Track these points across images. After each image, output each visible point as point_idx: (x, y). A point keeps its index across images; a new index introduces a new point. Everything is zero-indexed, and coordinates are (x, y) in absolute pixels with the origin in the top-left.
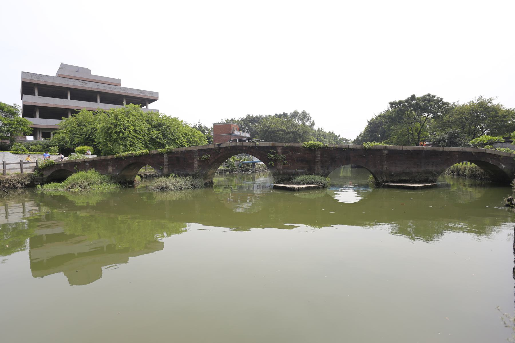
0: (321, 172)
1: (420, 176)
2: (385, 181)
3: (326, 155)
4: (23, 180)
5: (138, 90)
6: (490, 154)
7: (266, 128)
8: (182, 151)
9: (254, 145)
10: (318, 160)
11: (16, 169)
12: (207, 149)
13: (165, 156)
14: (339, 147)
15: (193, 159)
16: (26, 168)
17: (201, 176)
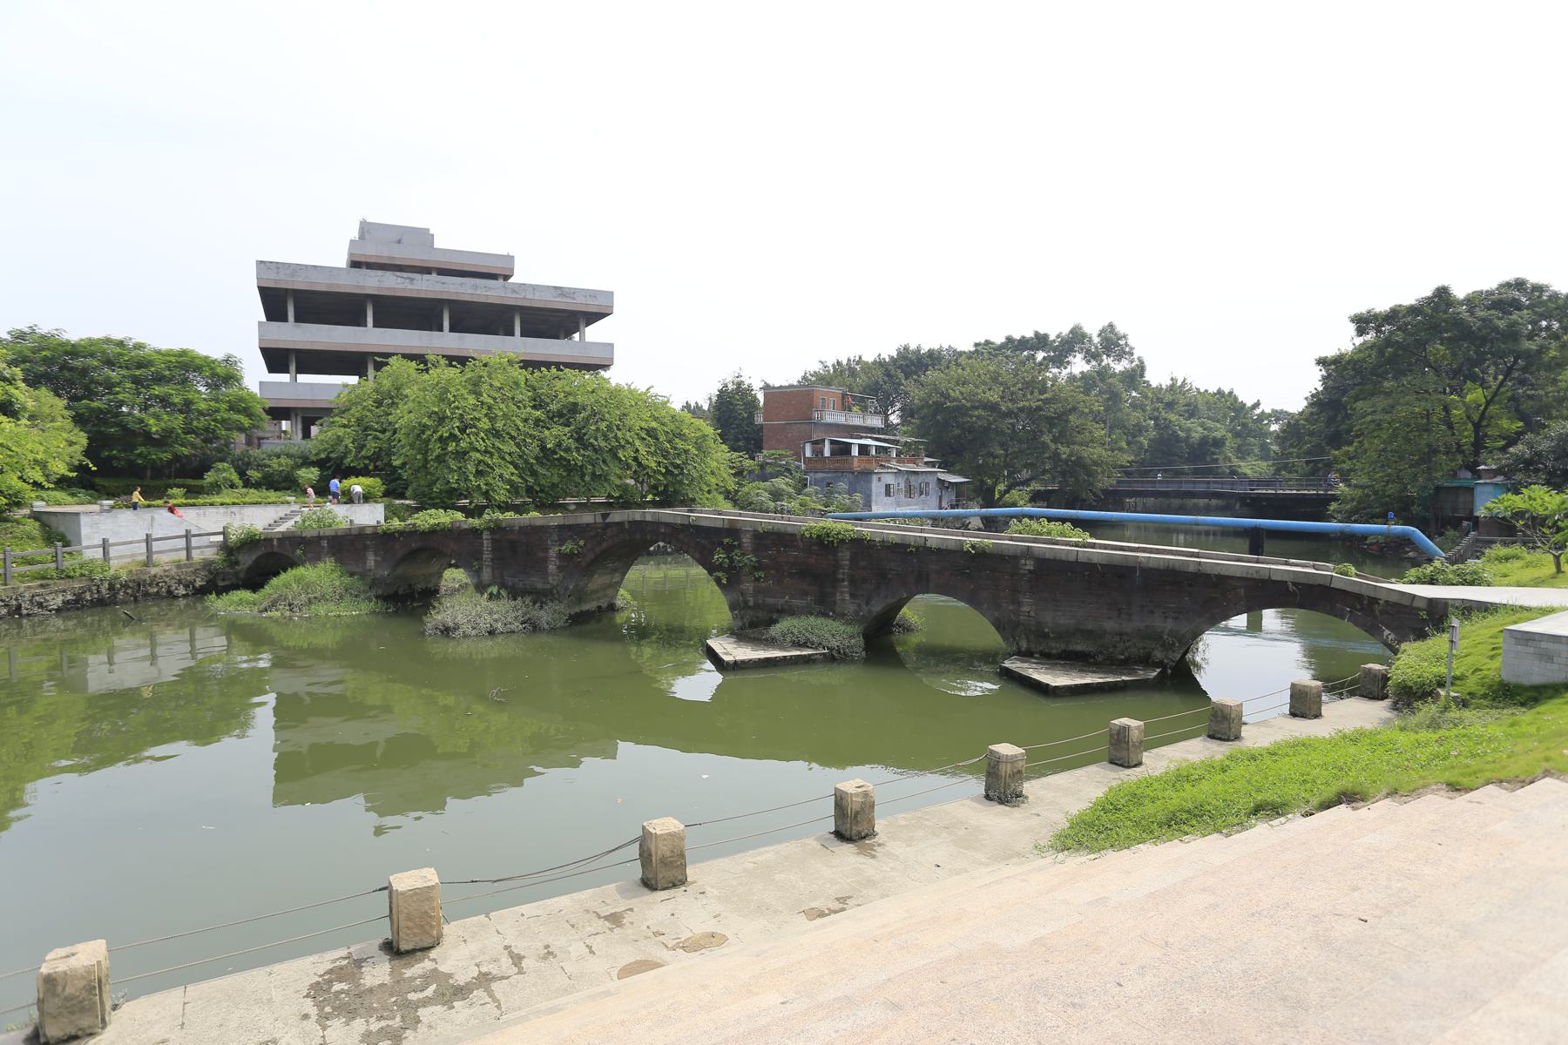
0: (851, 611)
1: (1128, 644)
2: (1023, 649)
3: (864, 563)
5: (555, 287)
6: (1345, 592)
7: (936, 398)
9: (686, 523)
10: (843, 573)
11: (177, 550)
12: (578, 526)
13: (486, 535)
15: (546, 550)
16: (199, 548)
17: (564, 595)
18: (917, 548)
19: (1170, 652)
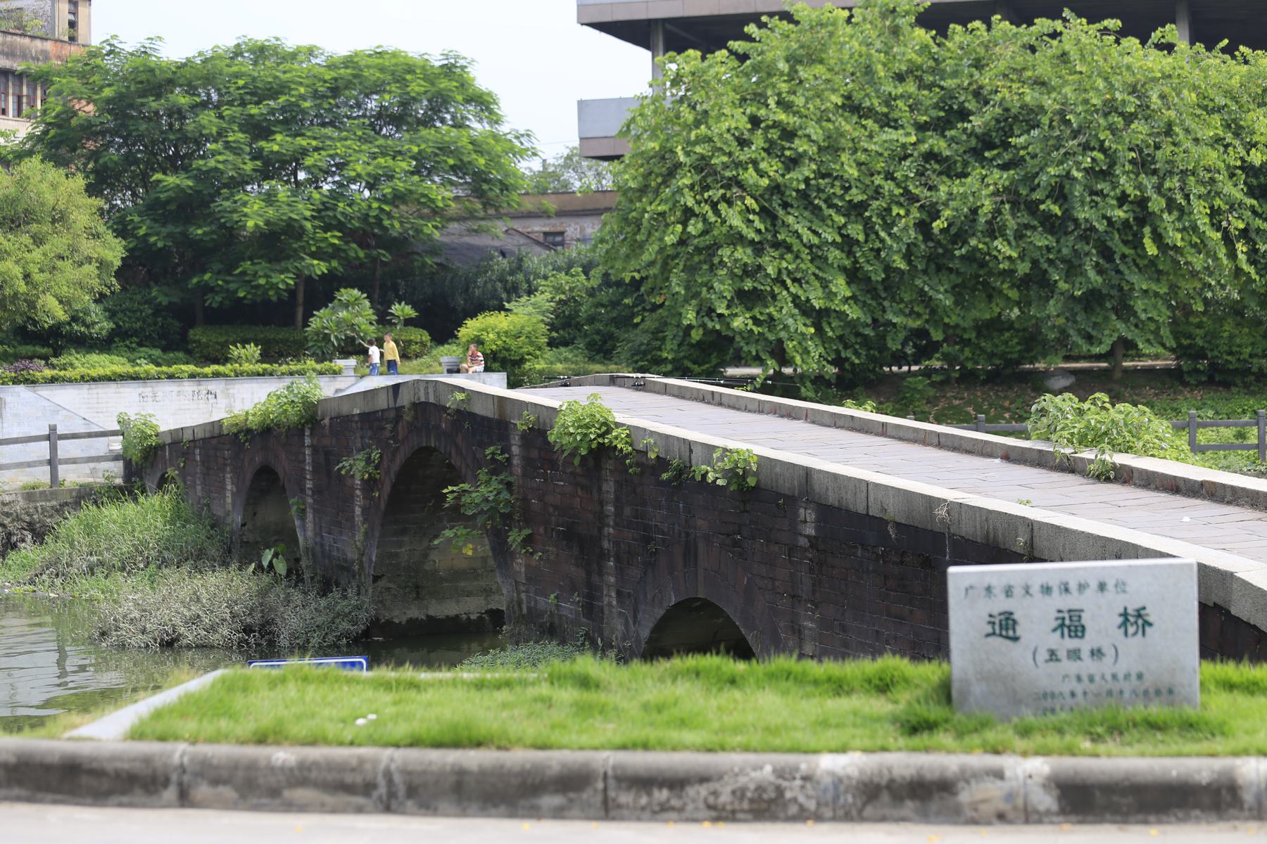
4: (51, 516)
8: (333, 416)
11: (29, 465)
16: (74, 461)
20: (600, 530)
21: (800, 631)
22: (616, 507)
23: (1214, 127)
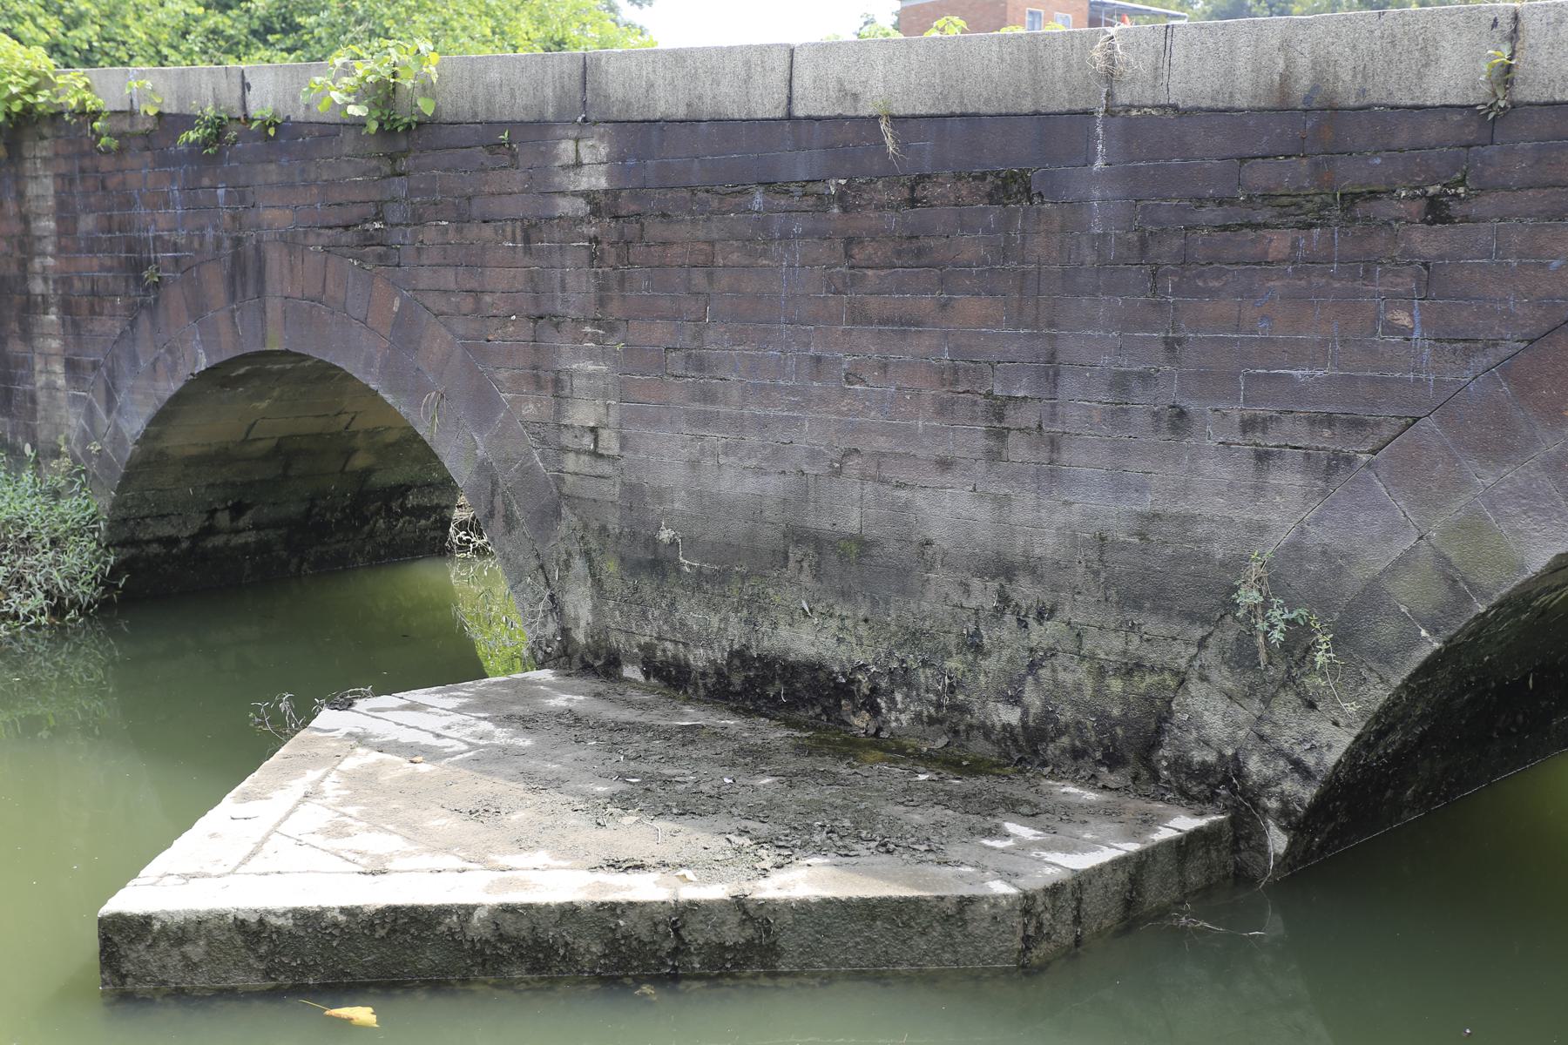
1: (1041, 634)
14: (174, 110)
18: (219, 128)
19: (1285, 709)
20: (23, 264)
21: (557, 383)
22: (60, 220)
23: (485, 27)
